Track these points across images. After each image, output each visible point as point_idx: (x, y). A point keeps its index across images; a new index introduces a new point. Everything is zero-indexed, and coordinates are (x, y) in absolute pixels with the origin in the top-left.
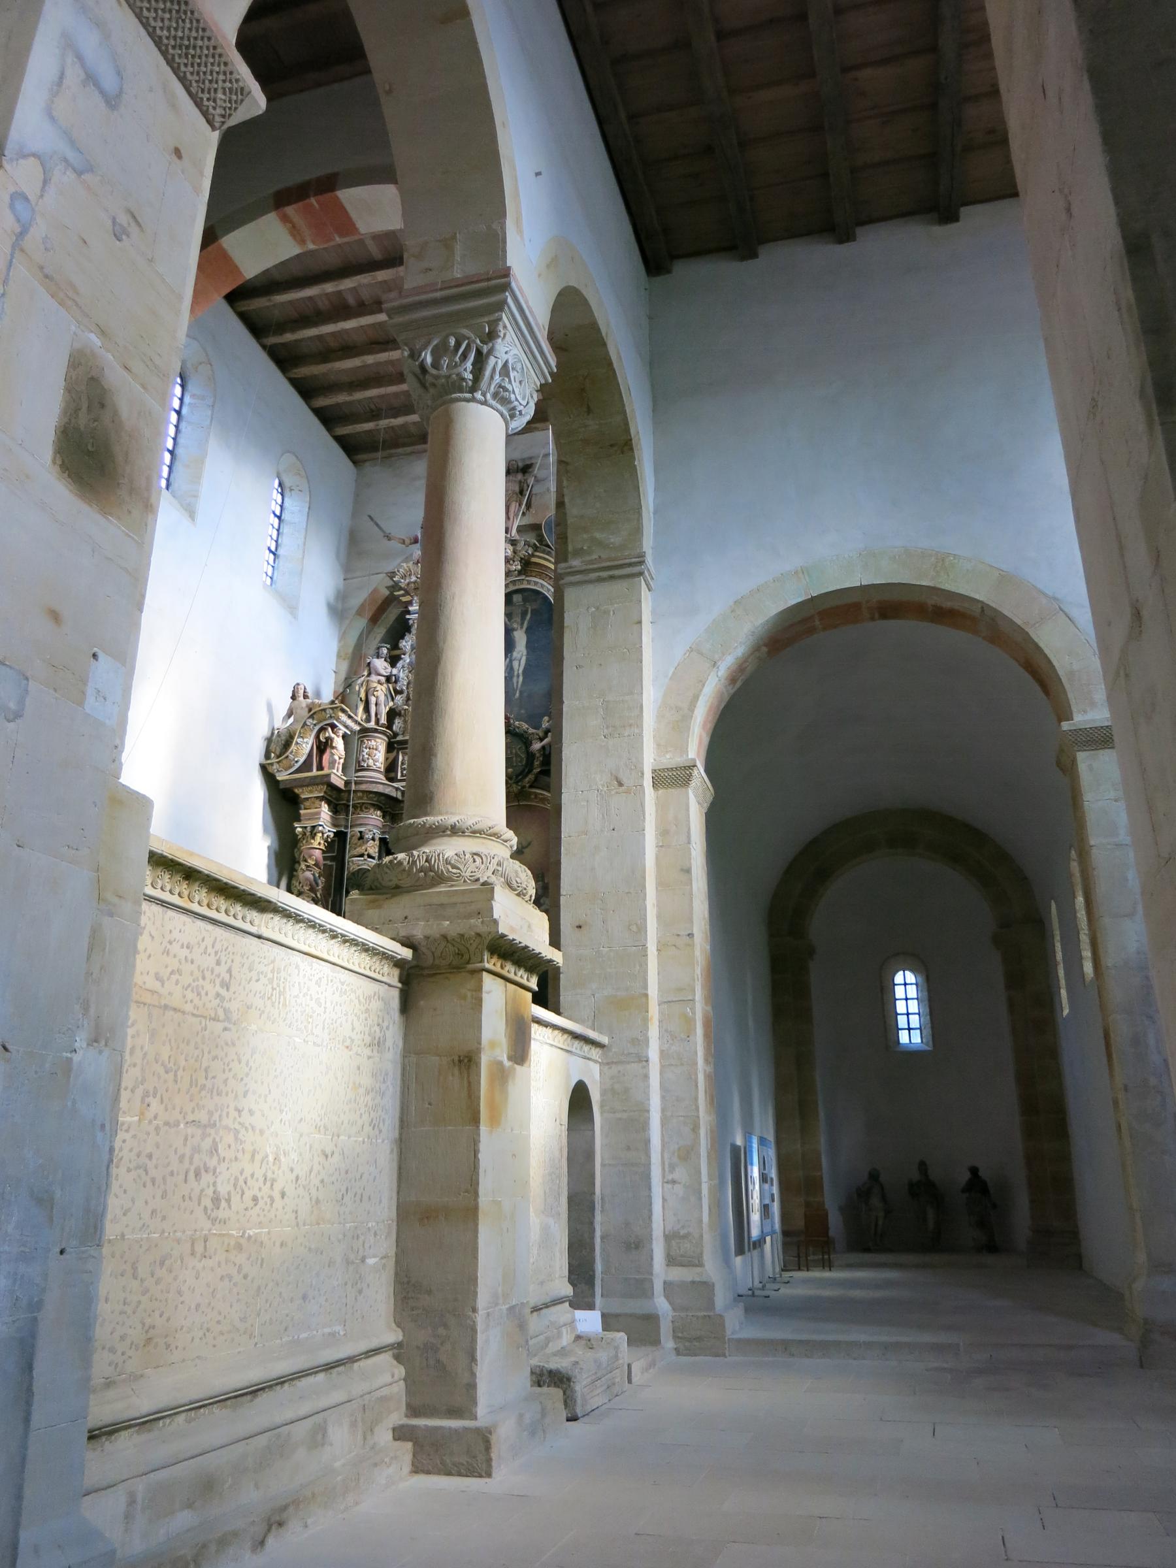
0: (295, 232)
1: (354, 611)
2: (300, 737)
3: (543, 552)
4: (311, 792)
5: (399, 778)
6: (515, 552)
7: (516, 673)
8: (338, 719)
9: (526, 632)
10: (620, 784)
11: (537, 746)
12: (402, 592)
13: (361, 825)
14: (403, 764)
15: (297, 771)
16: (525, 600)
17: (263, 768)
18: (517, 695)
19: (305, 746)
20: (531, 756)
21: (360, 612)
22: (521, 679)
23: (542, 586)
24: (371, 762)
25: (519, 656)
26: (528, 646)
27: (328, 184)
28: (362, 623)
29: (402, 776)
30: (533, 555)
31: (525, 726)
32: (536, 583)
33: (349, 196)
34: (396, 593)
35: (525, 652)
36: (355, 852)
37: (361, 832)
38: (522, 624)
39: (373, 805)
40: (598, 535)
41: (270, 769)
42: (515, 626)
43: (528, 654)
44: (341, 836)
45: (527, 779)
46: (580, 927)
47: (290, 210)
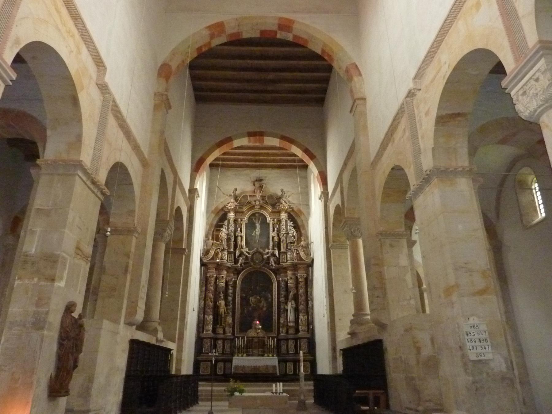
0: (249, 141)
1: (211, 212)
2: (211, 251)
3: (266, 204)
4: (212, 265)
5: (229, 261)
6: (259, 204)
7: (257, 235)
8: (221, 247)
9: (260, 224)
10: (346, 292)
11: (265, 256)
12: (226, 209)
13: (222, 274)
14: (230, 258)
15: (210, 260)
16: (260, 216)
17: (200, 258)
18: (257, 241)
19: (212, 253)
20: (263, 259)
21: (212, 212)
22: (258, 237)
23: (264, 213)
24: (225, 258)
25: (258, 230)
26: (261, 228)
27: (261, 134)
28: (213, 215)
29: (229, 261)
30: (263, 205)
31: (262, 251)
32: (263, 212)
33: (266, 138)
34: (224, 209)
35: (259, 230)
36: (221, 282)
37: (222, 276)
38: (259, 222)
39: (225, 269)
40: (338, 239)
41: (202, 259)
42: (257, 222)
43: (260, 231)
44: (217, 278)
45: (261, 264)
46: (340, 320)
47: (251, 138)
